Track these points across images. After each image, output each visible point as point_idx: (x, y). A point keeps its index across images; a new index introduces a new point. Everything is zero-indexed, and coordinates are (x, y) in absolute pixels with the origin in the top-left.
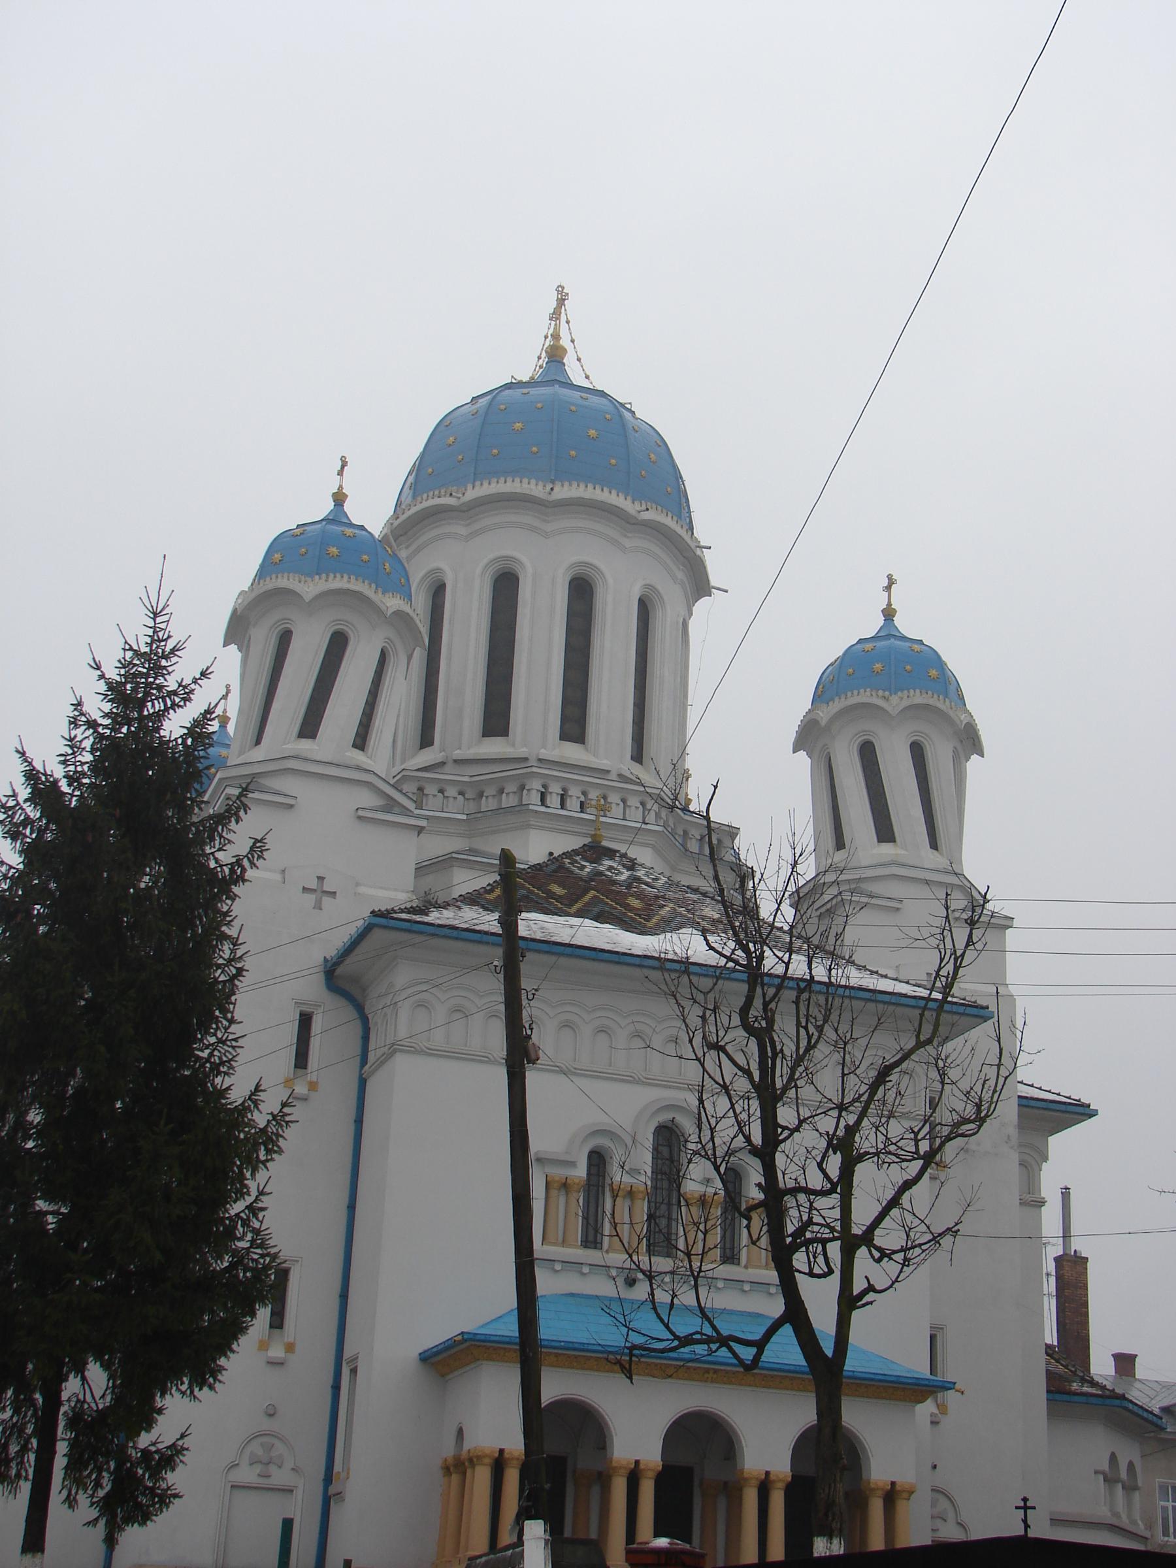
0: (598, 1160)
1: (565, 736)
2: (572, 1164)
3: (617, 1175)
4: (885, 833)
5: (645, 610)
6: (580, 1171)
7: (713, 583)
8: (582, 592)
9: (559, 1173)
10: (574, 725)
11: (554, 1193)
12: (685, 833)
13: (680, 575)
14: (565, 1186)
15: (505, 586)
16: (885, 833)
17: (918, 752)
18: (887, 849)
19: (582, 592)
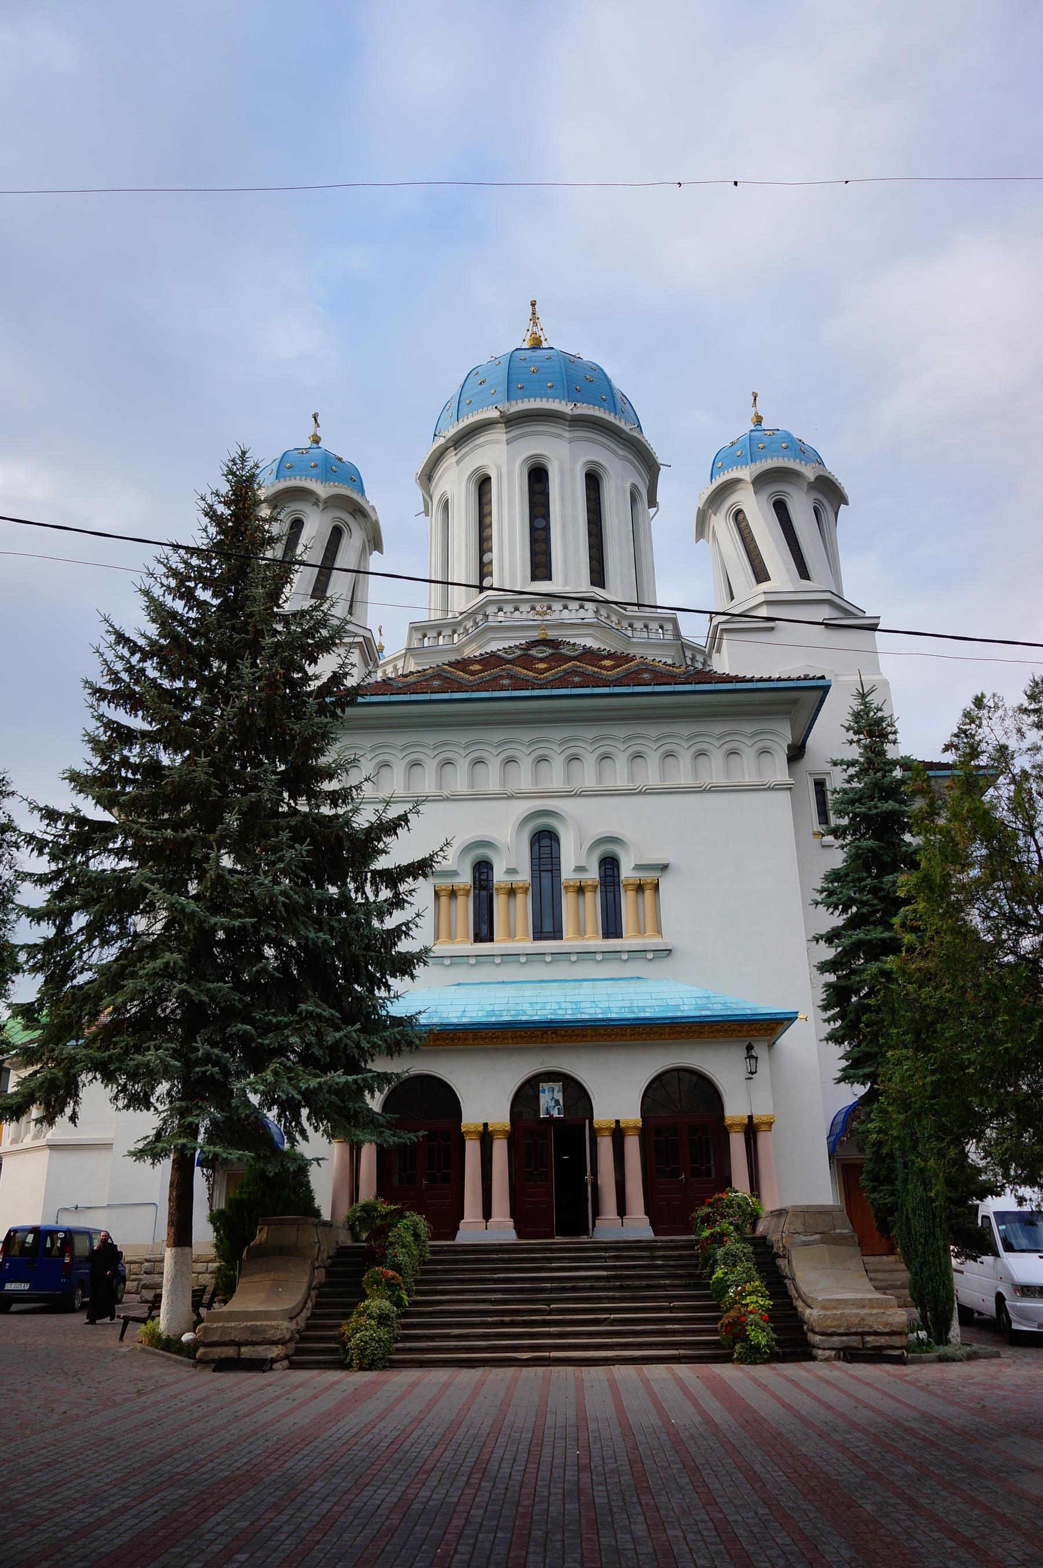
0: (482, 869)
1: (534, 578)
2: (453, 874)
3: (499, 876)
4: (761, 574)
5: (593, 481)
6: (466, 878)
7: (660, 461)
8: (538, 477)
9: (445, 883)
10: (541, 565)
11: (444, 900)
12: (631, 625)
13: (621, 452)
14: (453, 894)
15: (483, 484)
16: (761, 574)
17: (781, 508)
18: (765, 586)
19: (538, 477)
